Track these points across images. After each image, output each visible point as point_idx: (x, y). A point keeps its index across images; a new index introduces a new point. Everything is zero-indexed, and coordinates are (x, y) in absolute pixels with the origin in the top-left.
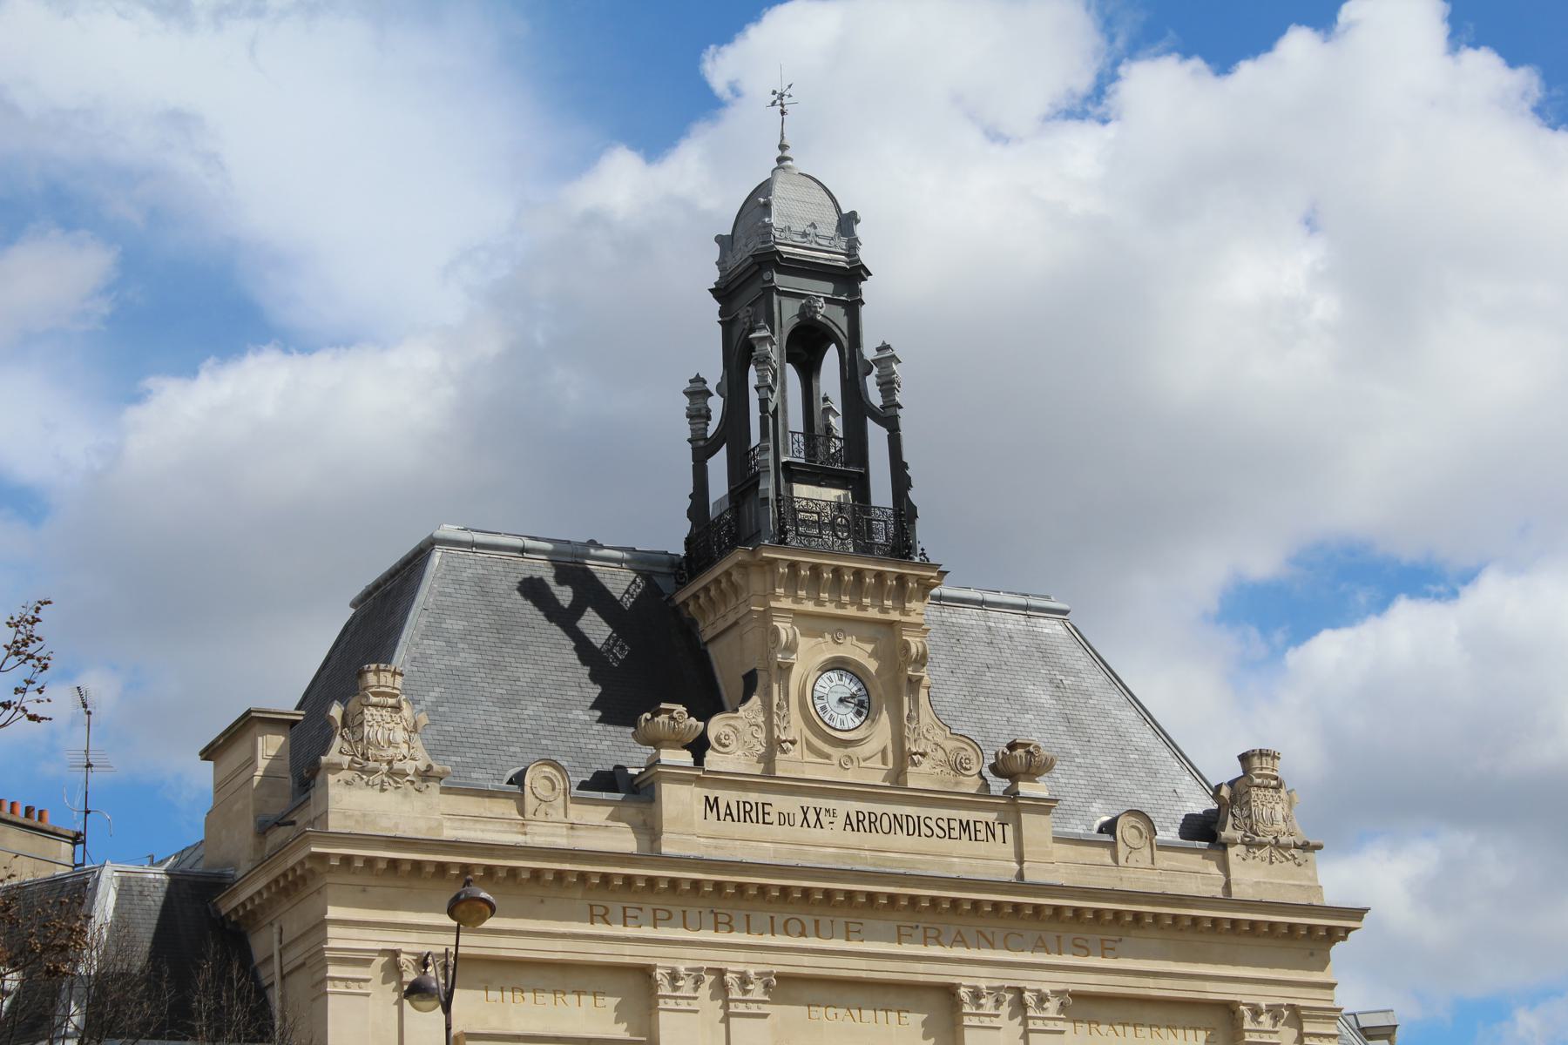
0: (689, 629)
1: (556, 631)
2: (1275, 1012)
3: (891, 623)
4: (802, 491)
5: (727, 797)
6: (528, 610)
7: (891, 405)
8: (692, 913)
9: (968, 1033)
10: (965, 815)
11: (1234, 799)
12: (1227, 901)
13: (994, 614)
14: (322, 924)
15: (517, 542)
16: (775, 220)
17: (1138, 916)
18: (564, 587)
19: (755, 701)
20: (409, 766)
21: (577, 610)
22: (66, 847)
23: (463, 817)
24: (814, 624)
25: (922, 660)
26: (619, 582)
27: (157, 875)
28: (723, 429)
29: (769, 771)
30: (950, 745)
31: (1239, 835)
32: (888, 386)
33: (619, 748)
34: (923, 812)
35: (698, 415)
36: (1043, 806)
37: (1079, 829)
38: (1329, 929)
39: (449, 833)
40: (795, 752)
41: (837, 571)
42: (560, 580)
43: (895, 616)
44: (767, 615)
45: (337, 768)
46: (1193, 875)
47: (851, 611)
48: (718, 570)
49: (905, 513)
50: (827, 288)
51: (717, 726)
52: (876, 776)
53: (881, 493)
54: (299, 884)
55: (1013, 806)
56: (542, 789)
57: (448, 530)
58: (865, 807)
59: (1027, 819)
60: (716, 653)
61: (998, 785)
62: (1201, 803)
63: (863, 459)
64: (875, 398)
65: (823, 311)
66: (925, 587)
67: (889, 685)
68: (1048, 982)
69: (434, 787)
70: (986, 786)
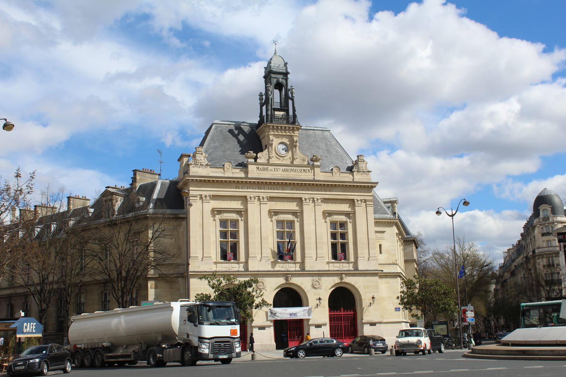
0: (258, 137)
1: (234, 139)
2: (361, 201)
3: (292, 136)
4: (276, 113)
5: (260, 167)
6: (230, 135)
7: (293, 97)
8: (254, 187)
9: (304, 206)
10: (304, 168)
11: (355, 164)
12: (353, 182)
13: (316, 131)
14: (189, 191)
15: (228, 123)
16: (272, 65)
17: (335, 185)
18: (237, 130)
19: (267, 150)
20: (204, 164)
21: (238, 134)
22: (157, 176)
23: (214, 172)
24: (277, 136)
25: (296, 142)
26: (246, 129)
27: (168, 181)
28: (265, 101)
29: (268, 162)
30: (302, 156)
31: (356, 170)
32: (292, 93)
33: (241, 158)
34: (296, 168)
35: (261, 99)
36: (318, 167)
37: (327, 170)
38: (372, 186)
39: (211, 175)
40: (273, 159)
41: (281, 127)
42: (236, 129)
43: (292, 134)
44: (268, 135)
45: (191, 164)
46: (347, 177)
47: (284, 134)
48: (261, 127)
49: (295, 116)
50: (282, 76)
51: (259, 155)
52: (288, 162)
53: (291, 113)
54: (186, 184)
55: (313, 167)
56: (228, 167)
57: (216, 121)
58: (286, 168)
59: (315, 169)
60: (262, 141)
61: (311, 163)
62: (350, 165)
63: (288, 106)
64: (290, 96)
65: (281, 80)
66: (298, 129)
67: (291, 147)
68: (319, 197)
69: (208, 167)
70: (309, 163)
